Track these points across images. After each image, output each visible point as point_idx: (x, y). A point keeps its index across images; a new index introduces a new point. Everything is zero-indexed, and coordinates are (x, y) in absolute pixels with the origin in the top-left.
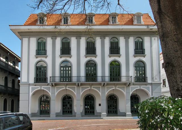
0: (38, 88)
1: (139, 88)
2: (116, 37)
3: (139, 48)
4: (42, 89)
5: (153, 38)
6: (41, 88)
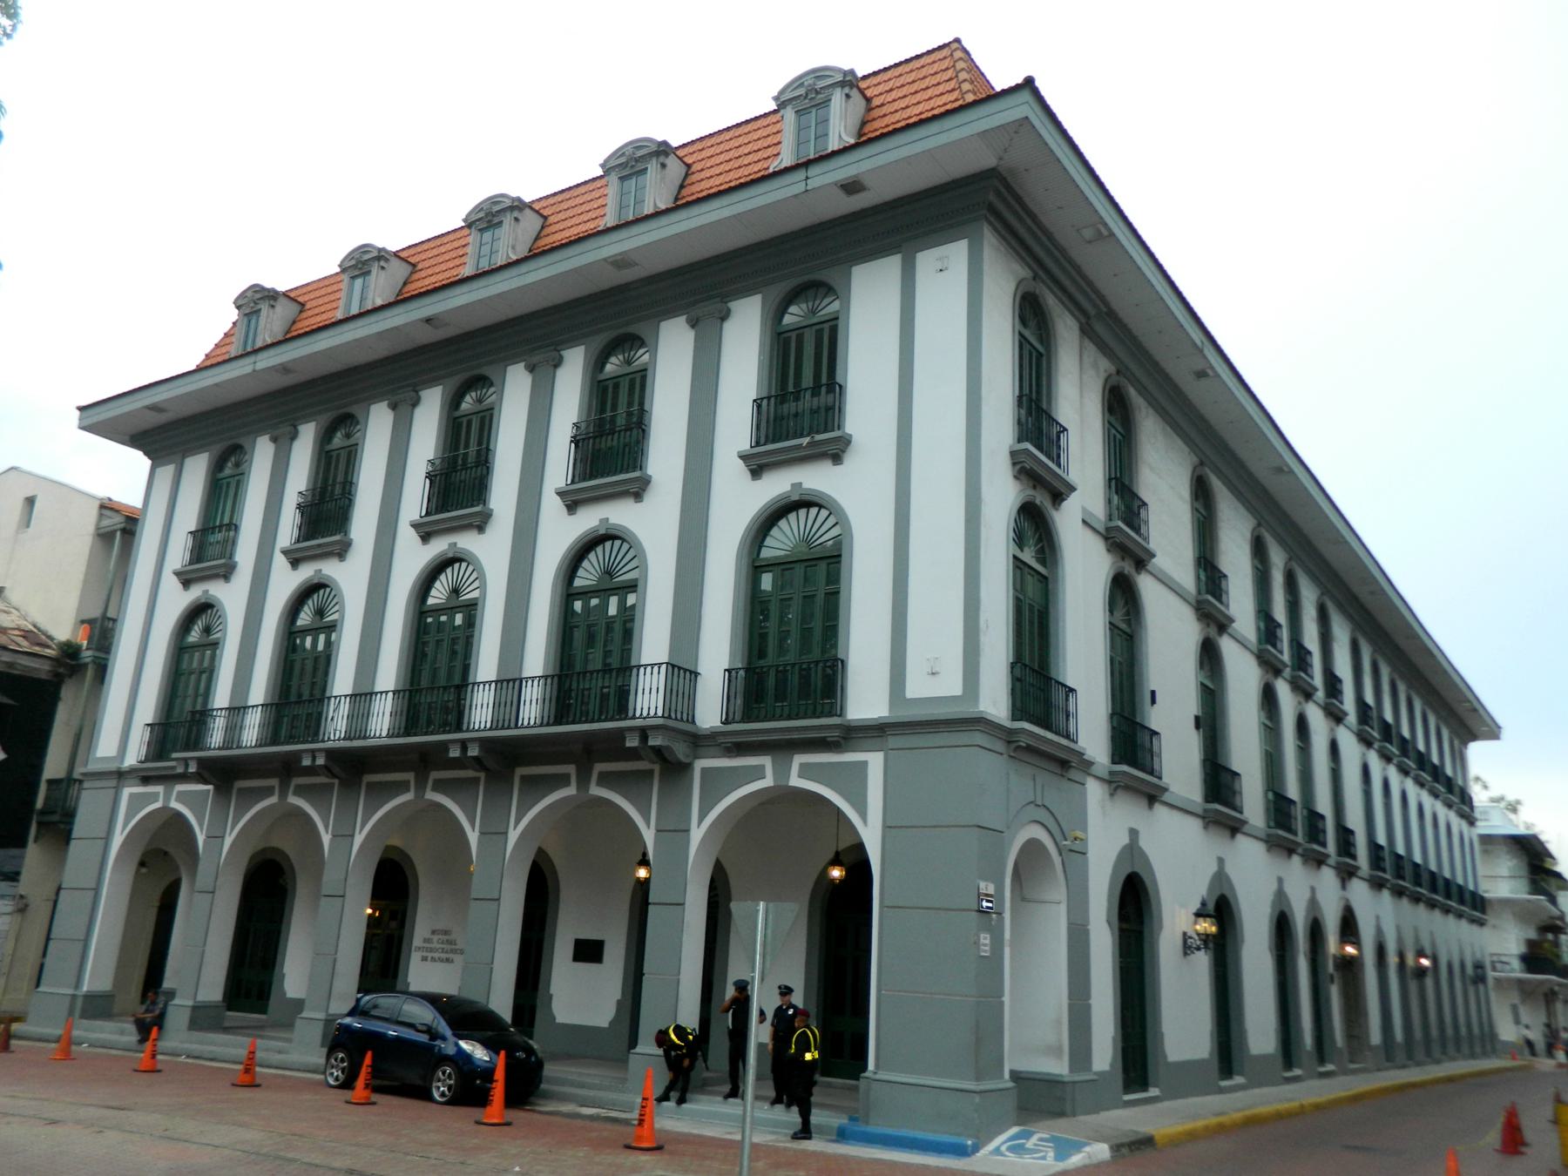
0: (154, 797)
1: (768, 782)
2: (631, 329)
3: (807, 380)
4: (174, 805)
5: (926, 260)
6: (167, 798)
